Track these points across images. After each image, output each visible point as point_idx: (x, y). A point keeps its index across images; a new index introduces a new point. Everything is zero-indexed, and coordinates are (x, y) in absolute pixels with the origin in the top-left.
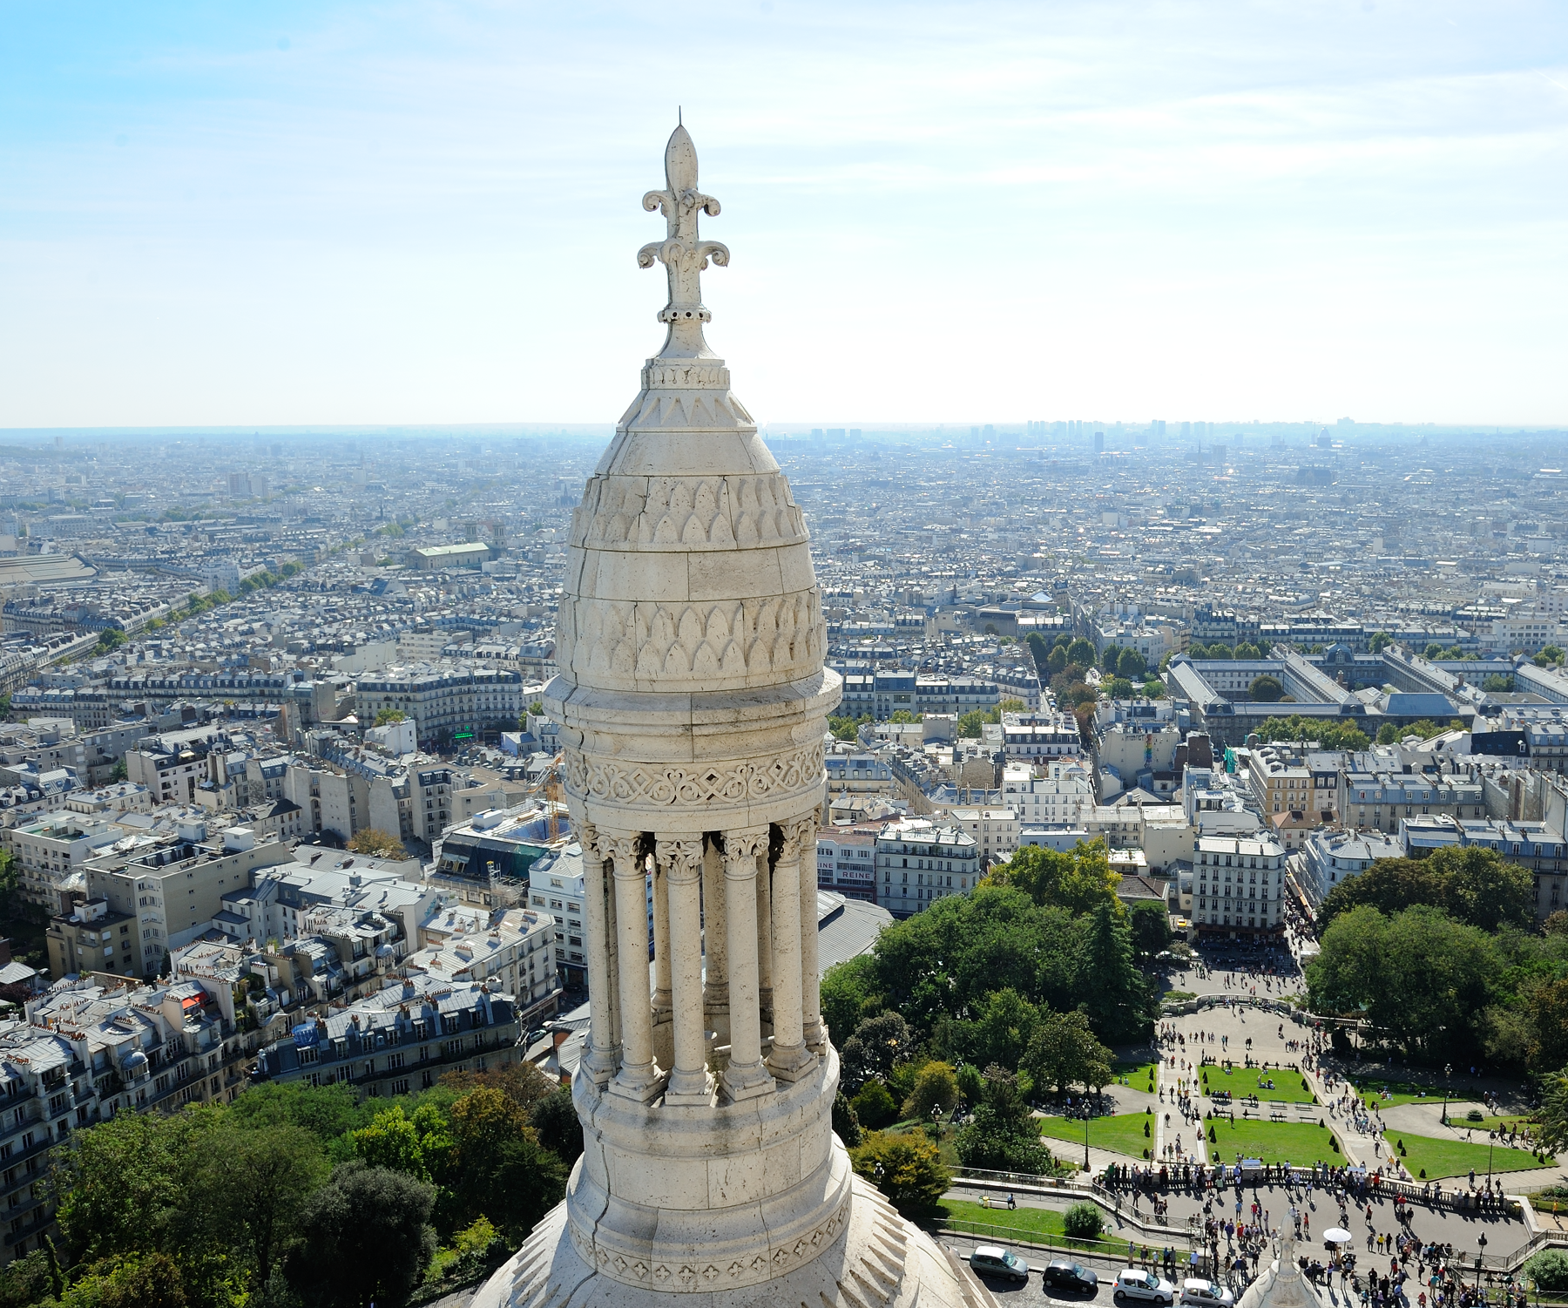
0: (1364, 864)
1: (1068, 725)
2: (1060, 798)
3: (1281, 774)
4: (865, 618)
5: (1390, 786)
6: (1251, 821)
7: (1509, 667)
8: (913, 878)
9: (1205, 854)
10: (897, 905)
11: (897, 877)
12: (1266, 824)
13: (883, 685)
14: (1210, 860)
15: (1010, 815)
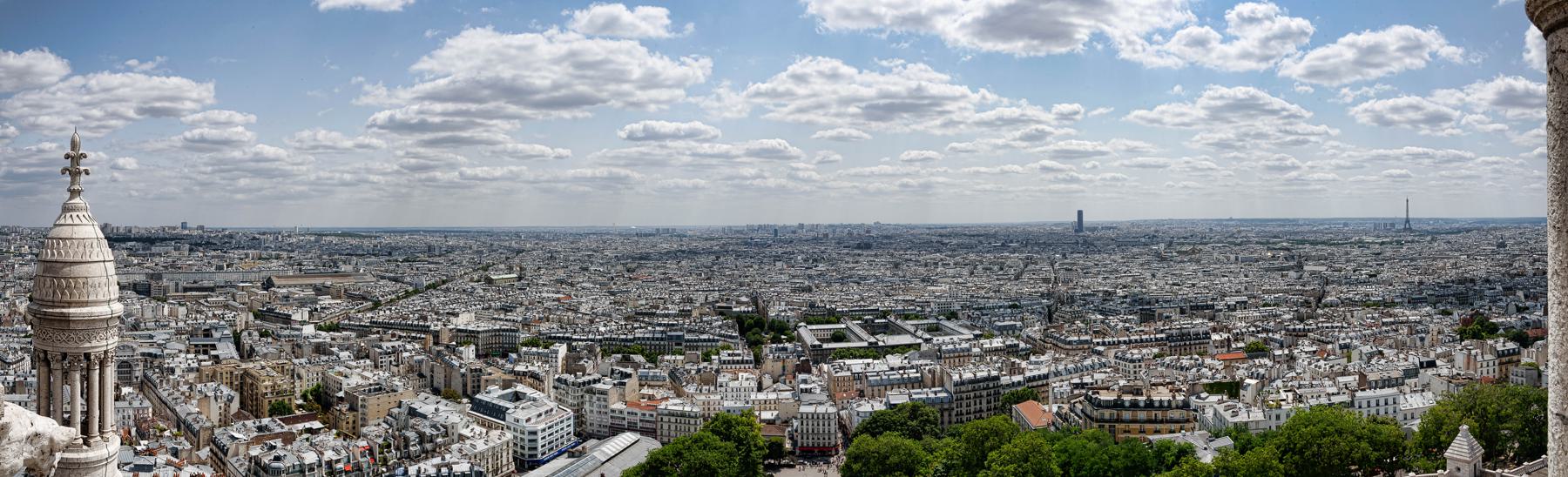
0: (871, 413)
1: (748, 355)
2: (742, 390)
3: (838, 374)
4: (667, 309)
5: (884, 377)
6: (824, 397)
7: (935, 321)
8: (673, 427)
9: (802, 414)
10: (666, 440)
11: (666, 426)
12: (831, 397)
13: (671, 338)
14: (805, 417)
15: (719, 397)
